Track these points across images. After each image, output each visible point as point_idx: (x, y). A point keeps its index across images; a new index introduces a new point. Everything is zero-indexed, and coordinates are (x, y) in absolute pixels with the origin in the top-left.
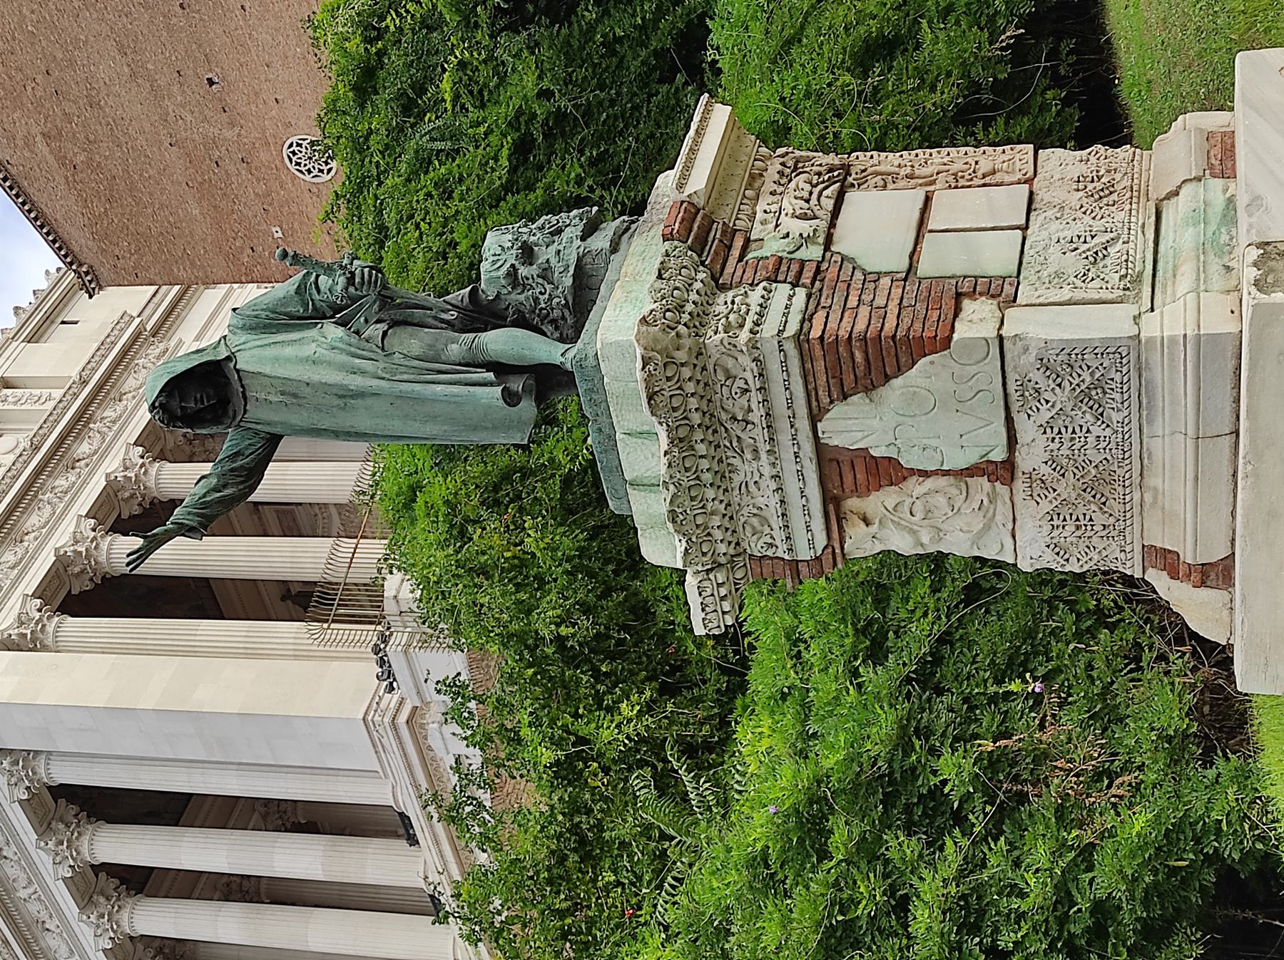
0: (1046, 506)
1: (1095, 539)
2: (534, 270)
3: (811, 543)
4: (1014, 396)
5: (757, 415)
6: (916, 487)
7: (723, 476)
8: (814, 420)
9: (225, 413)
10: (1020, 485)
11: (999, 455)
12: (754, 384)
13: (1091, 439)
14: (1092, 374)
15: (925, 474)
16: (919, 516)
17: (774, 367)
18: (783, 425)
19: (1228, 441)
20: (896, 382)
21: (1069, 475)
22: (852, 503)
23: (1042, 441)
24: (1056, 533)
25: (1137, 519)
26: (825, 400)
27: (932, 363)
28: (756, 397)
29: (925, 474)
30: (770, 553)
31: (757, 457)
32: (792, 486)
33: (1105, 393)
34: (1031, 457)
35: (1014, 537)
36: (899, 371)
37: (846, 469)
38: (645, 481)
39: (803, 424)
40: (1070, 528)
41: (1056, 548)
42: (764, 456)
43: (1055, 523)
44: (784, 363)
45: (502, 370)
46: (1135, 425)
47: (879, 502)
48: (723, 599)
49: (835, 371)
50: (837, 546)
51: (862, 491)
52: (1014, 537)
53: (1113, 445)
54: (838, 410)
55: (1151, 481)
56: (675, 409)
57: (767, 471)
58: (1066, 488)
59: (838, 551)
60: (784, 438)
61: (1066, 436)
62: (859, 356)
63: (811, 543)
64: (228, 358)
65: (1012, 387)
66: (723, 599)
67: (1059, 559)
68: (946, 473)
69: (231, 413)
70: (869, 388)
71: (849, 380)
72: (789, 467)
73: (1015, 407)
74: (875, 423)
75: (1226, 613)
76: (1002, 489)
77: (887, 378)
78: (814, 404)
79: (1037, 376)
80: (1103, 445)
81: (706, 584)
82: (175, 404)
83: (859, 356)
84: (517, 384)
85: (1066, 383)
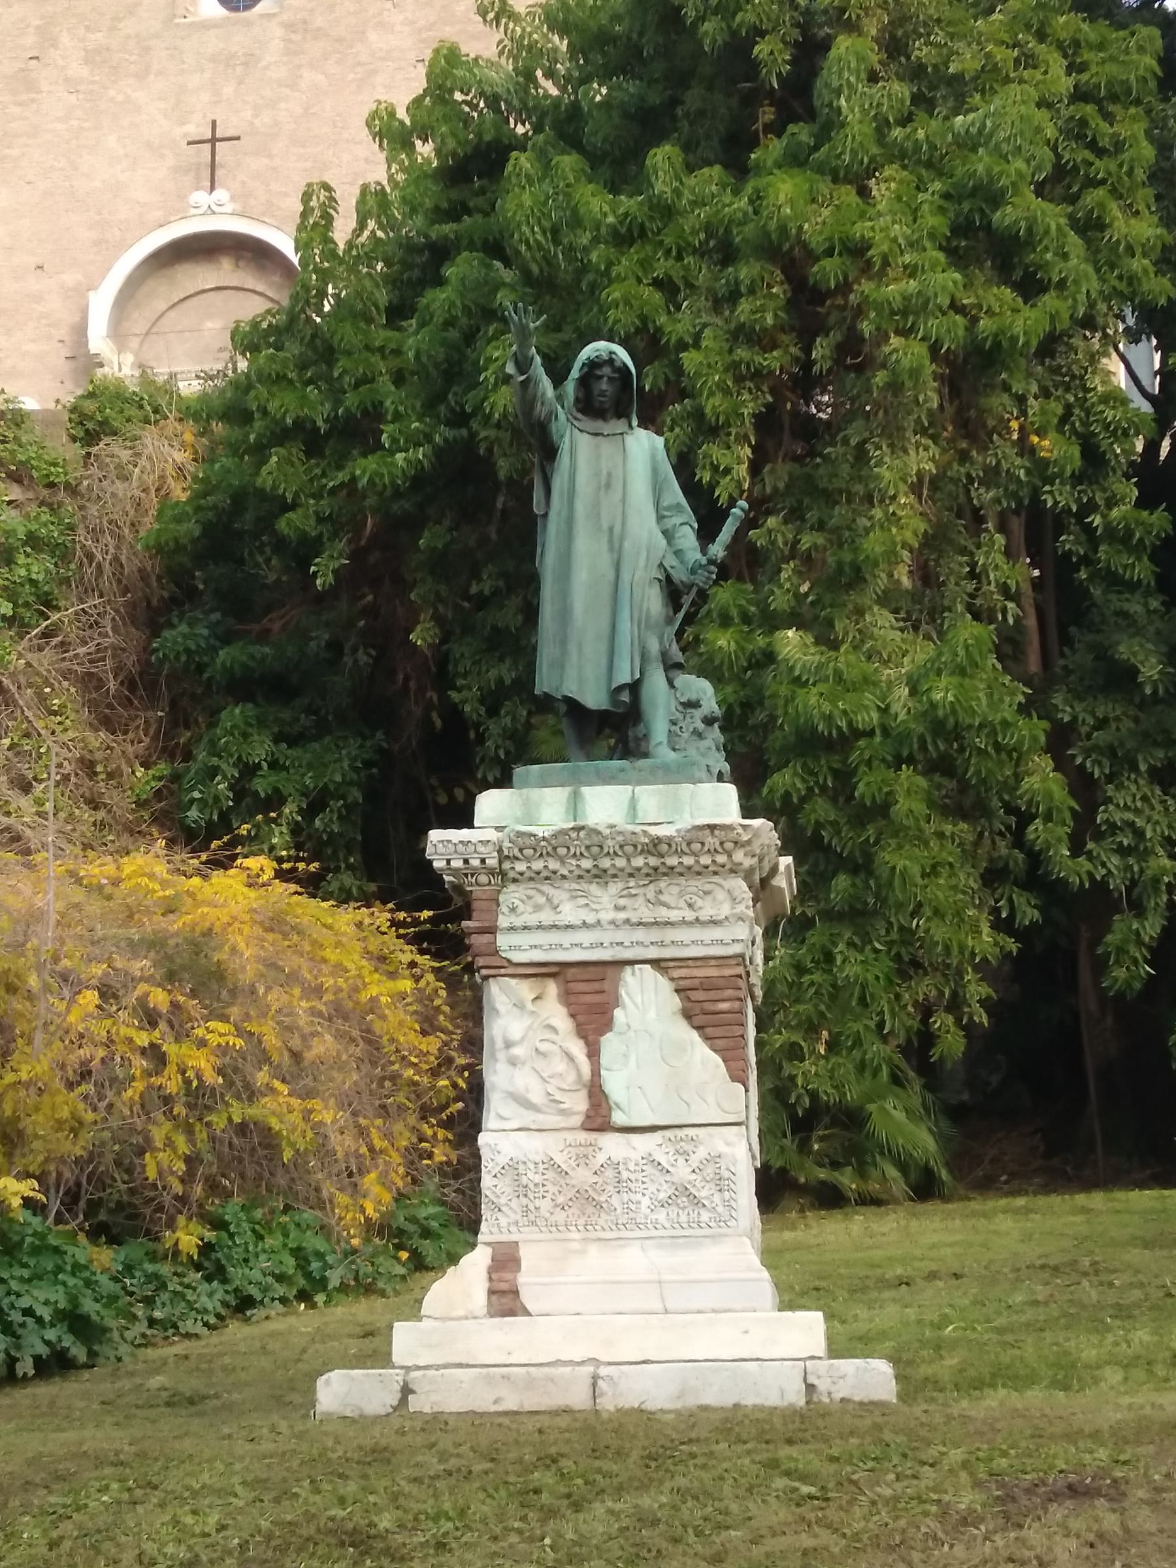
0: (559, 1159)
1: (524, 1201)
2: (701, 726)
3: (519, 948)
4: (681, 1133)
5: (663, 914)
6: (578, 1049)
7: (600, 876)
8: (655, 963)
9: (579, 411)
10: (583, 1136)
11: (618, 1118)
12: (704, 915)
13: (639, 1196)
14: (707, 1198)
15: (594, 1053)
16: (543, 1047)
17: (717, 933)
18: (655, 935)
19: (658, 1306)
20: (695, 1035)
21: (595, 1179)
22: (552, 988)
23: (635, 1156)
24: (532, 1166)
25: (549, 1236)
26: (676, 974)
27: (718, 1066)
28: (690, 916)
29: (594, 1053)
30: (504, 909)
31: (617, 908)
32: (585, 937)
33: (684, 1208)
34: (612, 1145)
35: (519, 1130)
36: (707, 1039)
37: (596, 986)
38: (579, 806)
39: (653, 953)
40: (538, 1179)
41: (512, 1168)
42: (622, 916)
43: (541, 1166)
44: (721, 942)
45: (635, 687)
46: (654, 1233)
47: (556, 1014)
48: (466, 861)
49: (707, 985)
50: (510, 971)
51: (567, 997)
52: (519, 1130)
53: (632, 1215)
54: (664, 985)
55: (593, 1249)
56: (689, 844)
57: (607, 916)
58: (582, 1177)
59: (503, 971)
60: (640, 935)
61: (640, 1176)
62: (724, 1006)
63: (519, 948)
64: (631, 427)
65: (691, 1132)
66: (466, 861)
67: (498, 1168)
68: (596, 1073)
69: (579, 416)
70: (688, 1015)
71: (699, 995)
72: (607, 936)
73: (668, 1133)
74: (652, 1014)
75: (461, 1313)
76: (577, 1120)
77: (699, 1028)
78: (672, 964)
79: (702, 1153)
80: (633, 1207)
81: (490, 847)
82: (606, 370)
83: (724, 1006)
84: (625, 697)
85: (694, 1176)
